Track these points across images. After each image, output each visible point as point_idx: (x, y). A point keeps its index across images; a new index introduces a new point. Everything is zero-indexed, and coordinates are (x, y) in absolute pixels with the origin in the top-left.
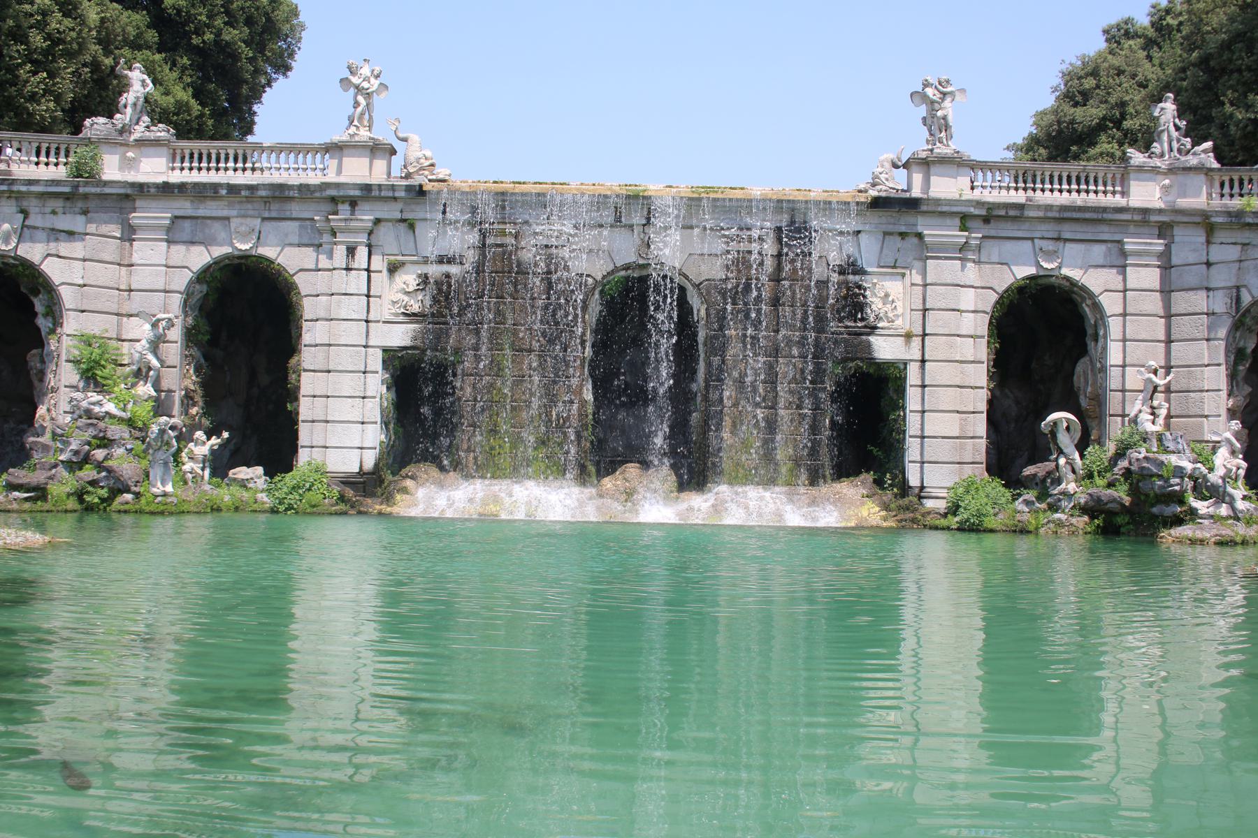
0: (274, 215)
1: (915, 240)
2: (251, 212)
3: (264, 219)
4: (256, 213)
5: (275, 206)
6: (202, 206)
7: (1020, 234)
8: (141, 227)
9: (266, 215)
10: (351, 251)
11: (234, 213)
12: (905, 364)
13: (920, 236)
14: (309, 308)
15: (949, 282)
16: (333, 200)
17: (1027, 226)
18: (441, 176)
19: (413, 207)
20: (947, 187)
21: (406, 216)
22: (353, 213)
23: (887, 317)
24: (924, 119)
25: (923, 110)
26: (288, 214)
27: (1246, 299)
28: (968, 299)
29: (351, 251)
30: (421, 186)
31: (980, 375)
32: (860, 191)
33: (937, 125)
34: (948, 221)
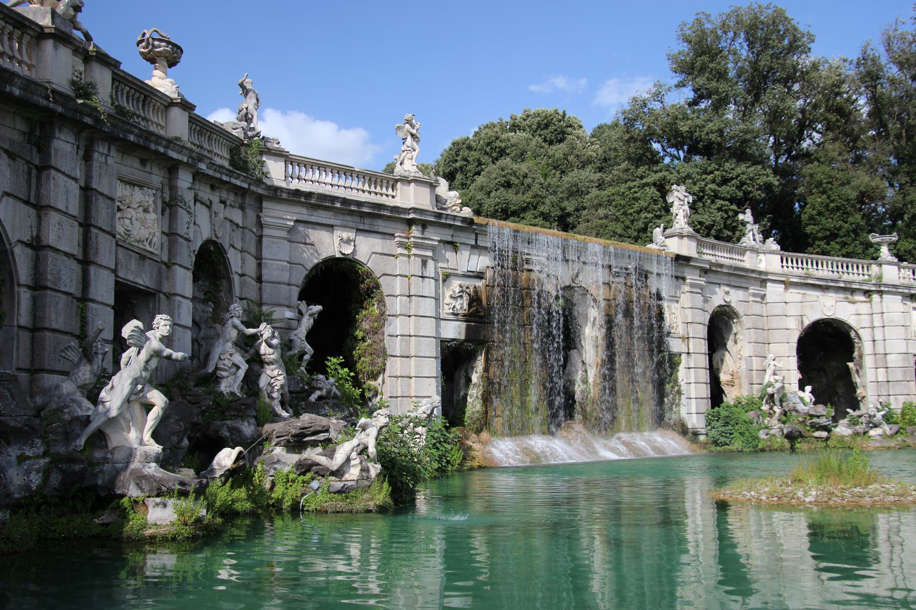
0: (366, 227)
2: (350, 224)
3: (358, 230)
4: (350, 224)
5: (367, 221)
6: (315, 213)
8: (270, 226)
9: (361, 227)
10: (424, 263)
11: (338, 223)
14: (395, 305)
16: (410, 223)
17: (719, 276)
21: (455, 239)
22: (423, 233)
26: (376, 229)
27: (807, 323)
29: (424, 263)
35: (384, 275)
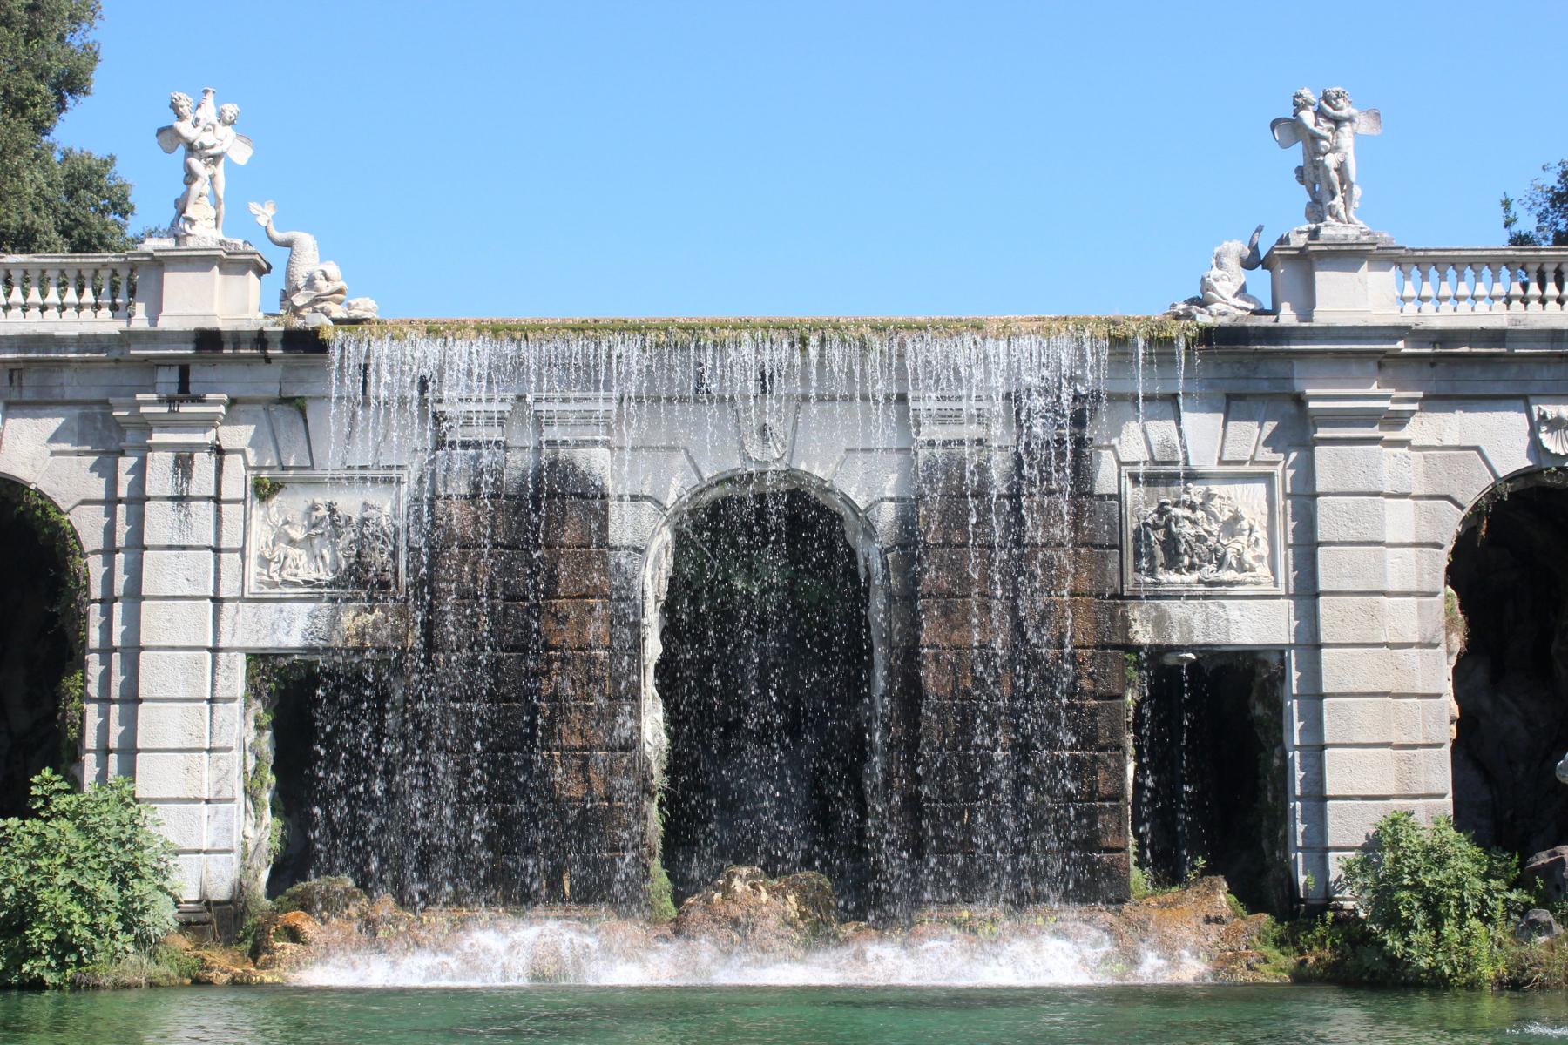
0: (28, 395)
1: (1291, 408)
7: (1499, 389)
9: (15, 397)
12: (1282, 652)
13: (1300, 400)
15: (1361, 487)
17: (1514, 370)
18: (356, 313)
19: (303, 373)
20: (1352, 299)
23: (1240, 560)
24: (1300, 172)
25: (1296, 155)
28: (1400, 520)
30: (316, 331)
31: (1436, 671)
32: (1177, 317)
33: (1320, 187)
34: (1354, 369)
35: (84, 502)
